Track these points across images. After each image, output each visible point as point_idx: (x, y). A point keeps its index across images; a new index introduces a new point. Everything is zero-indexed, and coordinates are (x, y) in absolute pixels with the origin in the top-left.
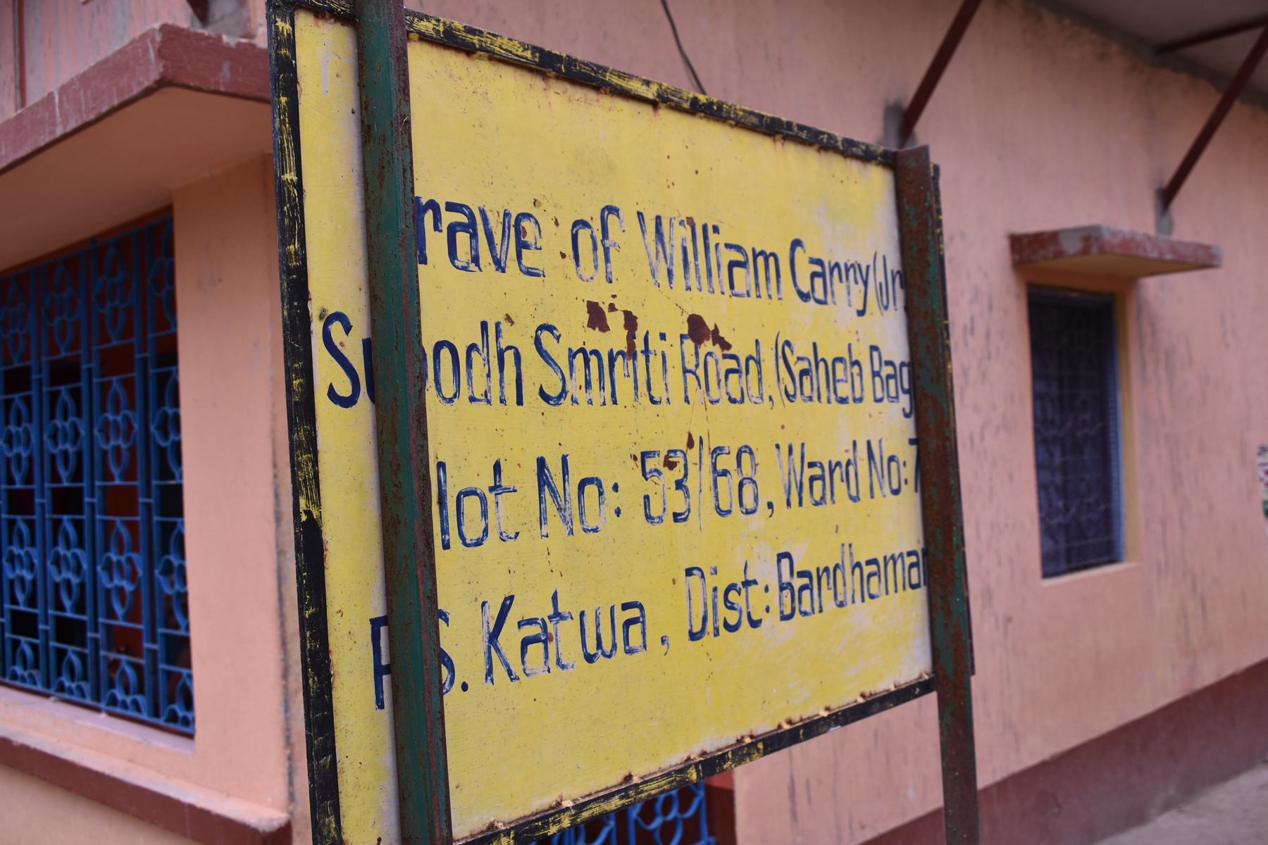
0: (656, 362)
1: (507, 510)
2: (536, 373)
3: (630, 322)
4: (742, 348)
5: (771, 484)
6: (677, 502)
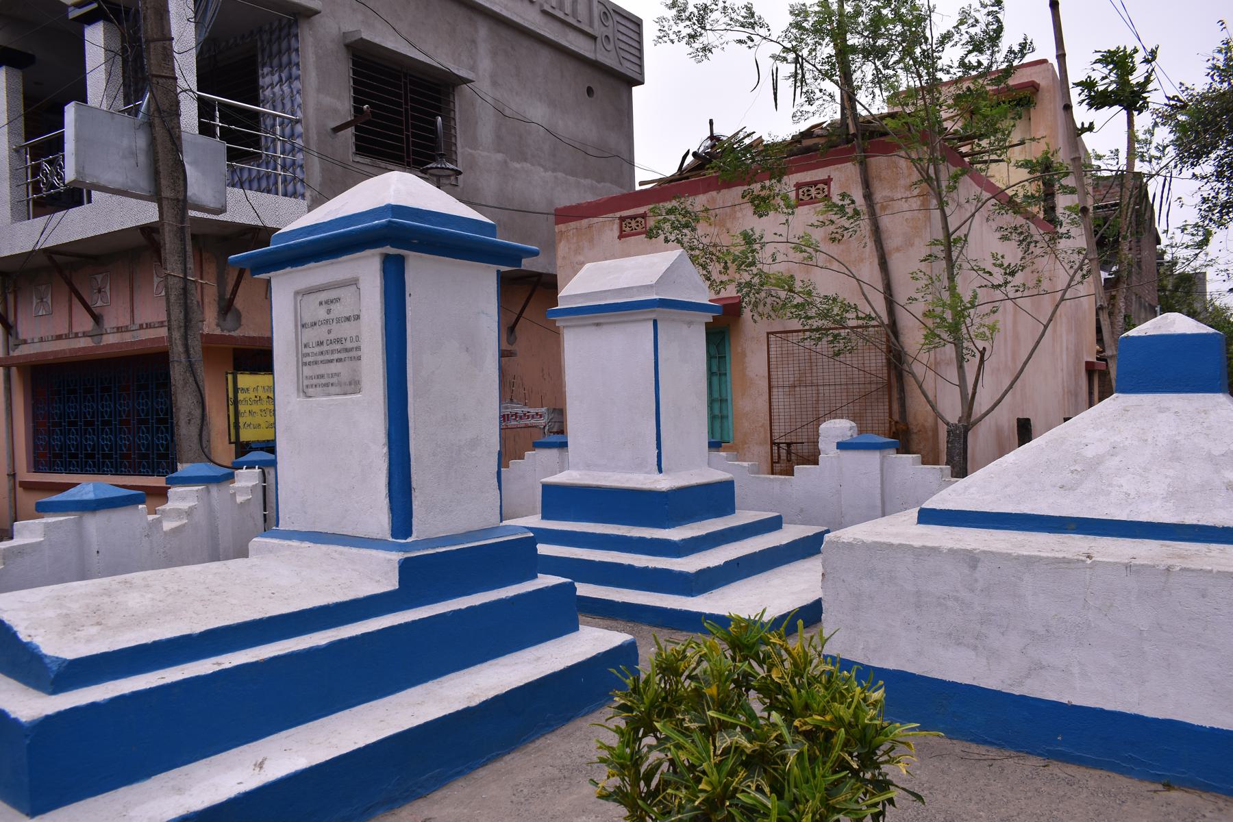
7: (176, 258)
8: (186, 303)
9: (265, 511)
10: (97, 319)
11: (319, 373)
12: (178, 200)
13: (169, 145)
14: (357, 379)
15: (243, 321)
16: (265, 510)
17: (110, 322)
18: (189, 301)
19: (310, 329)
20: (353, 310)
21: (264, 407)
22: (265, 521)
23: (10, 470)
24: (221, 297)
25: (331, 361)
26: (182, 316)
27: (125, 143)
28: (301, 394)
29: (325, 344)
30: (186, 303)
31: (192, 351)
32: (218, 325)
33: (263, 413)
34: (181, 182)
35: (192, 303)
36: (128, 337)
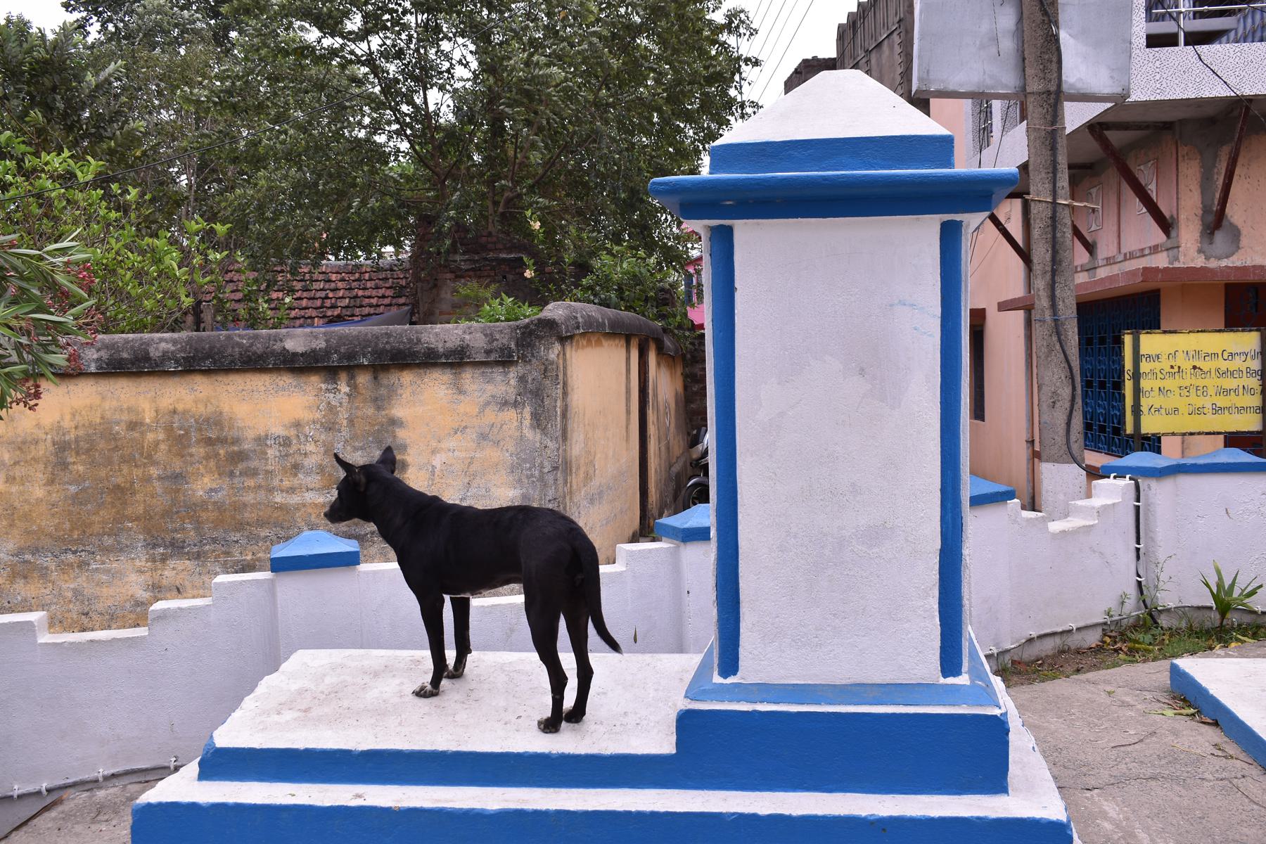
0: (1184, 373)
1: (1152, 394)
2: (1159, 375)
3: (1179, 367)
4: (1206, 369)
5: (1212, 391)
6: (1188, 394)
7: (1043, 175)
8: (1054, 237)
9: (1138, 543)
10: (1090, 247)
12: (1049, 93)
13: (1039, 16)
15: (1244, 241)
16: (1138, 543)
17: (1104, 251)
18: (1058, 235)
21: (1187, 383)
22: (1138, 557)
23: (1029, 435)
24: (1206, 210)
26: (1048, 256)
27: (985, 27)
30: (1054, 237)
31: (1061, 305)
32: (1200, 251)
33: (1185, 392)
34: (1054, 66)
35: (1063, 237)
36: (1115, 270)
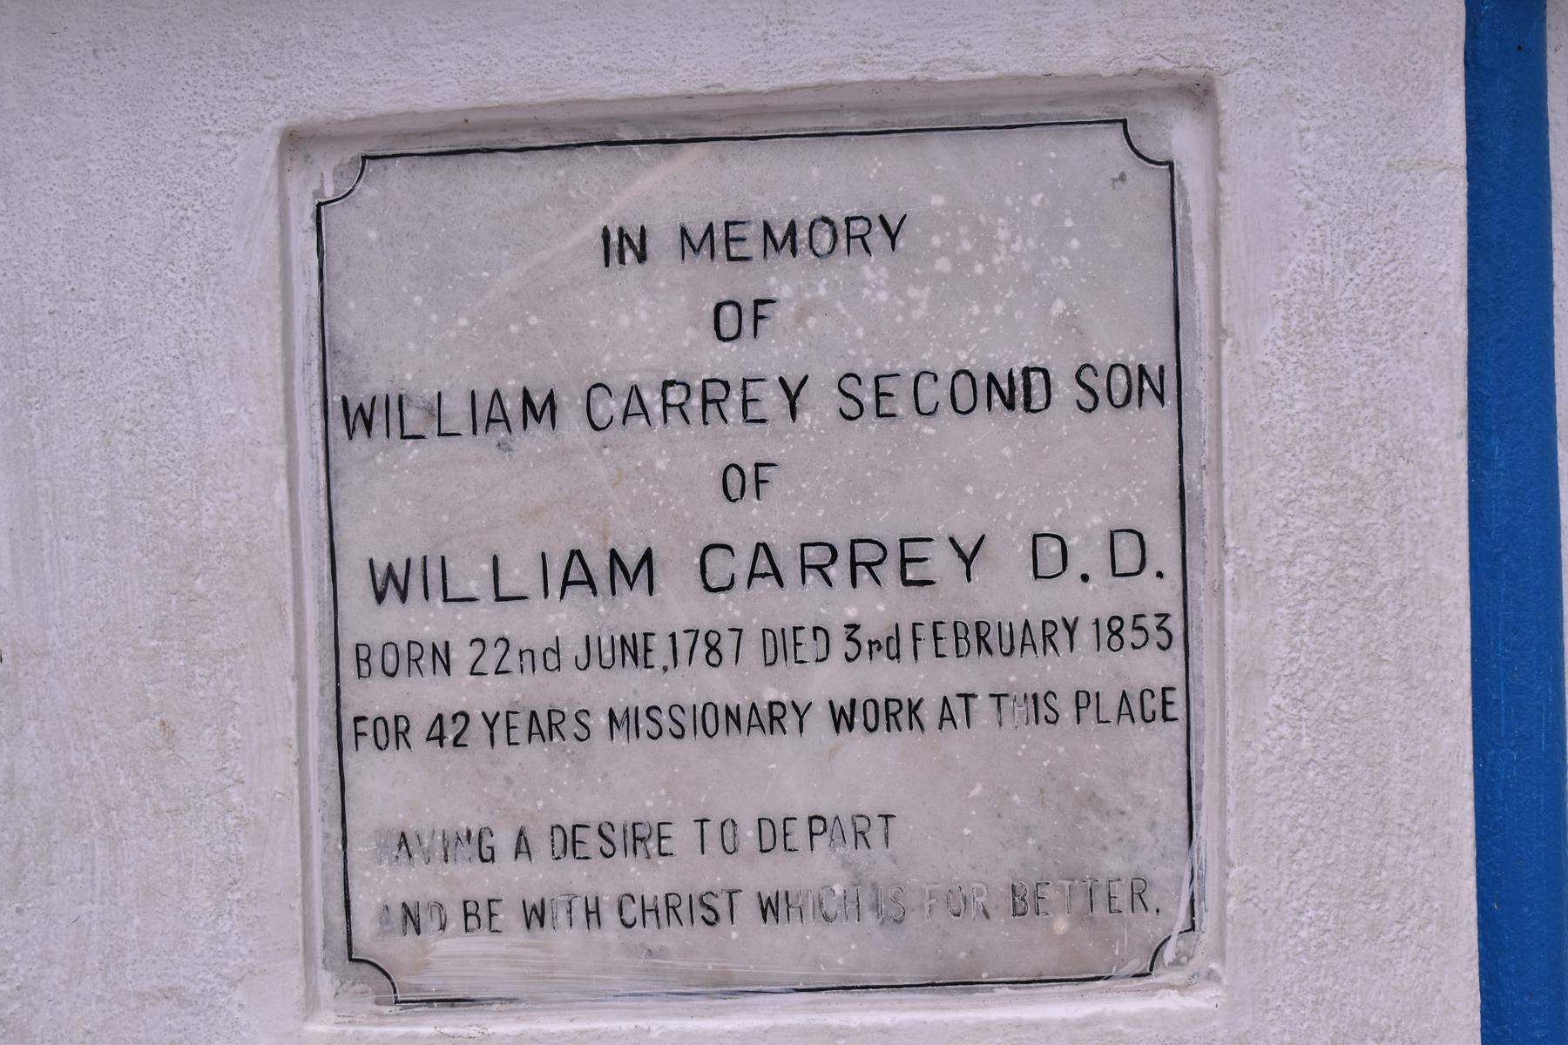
11: (589, 808)
14: (1114, 865)
19: (467, 446)
20: (1070, 324)
25: (773, 718)
28: (326, 982)
29: (676, 577)
